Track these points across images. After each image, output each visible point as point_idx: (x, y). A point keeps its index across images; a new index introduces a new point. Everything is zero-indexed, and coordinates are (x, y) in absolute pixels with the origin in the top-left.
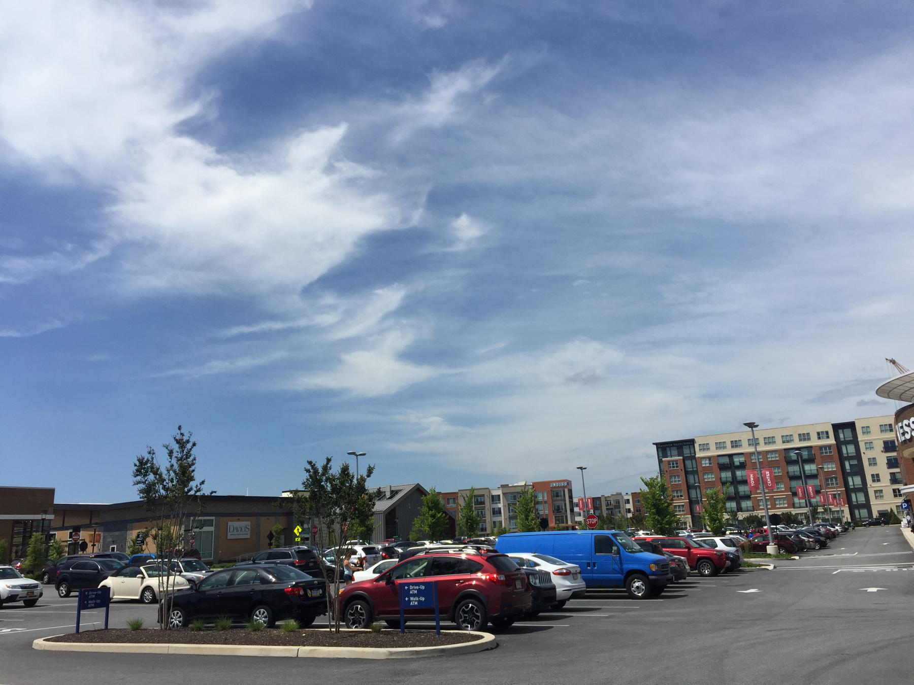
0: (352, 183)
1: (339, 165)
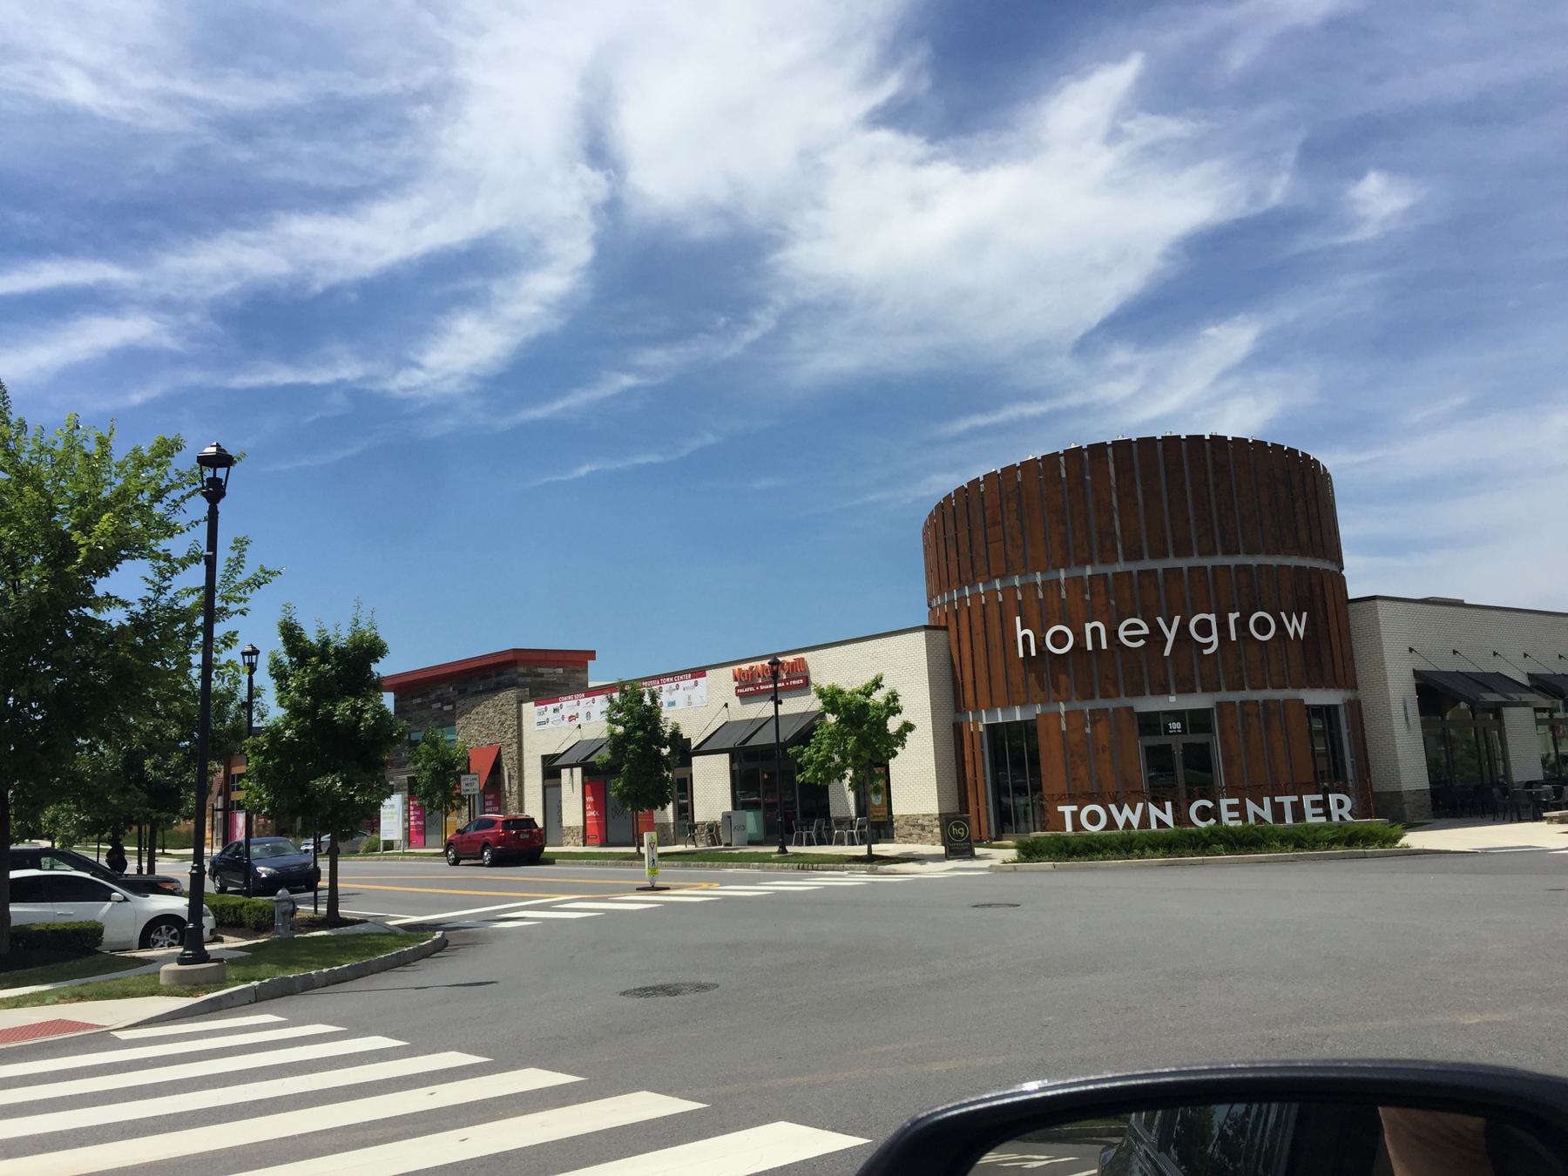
0: (1153, 152)
1: (1128, 126)
